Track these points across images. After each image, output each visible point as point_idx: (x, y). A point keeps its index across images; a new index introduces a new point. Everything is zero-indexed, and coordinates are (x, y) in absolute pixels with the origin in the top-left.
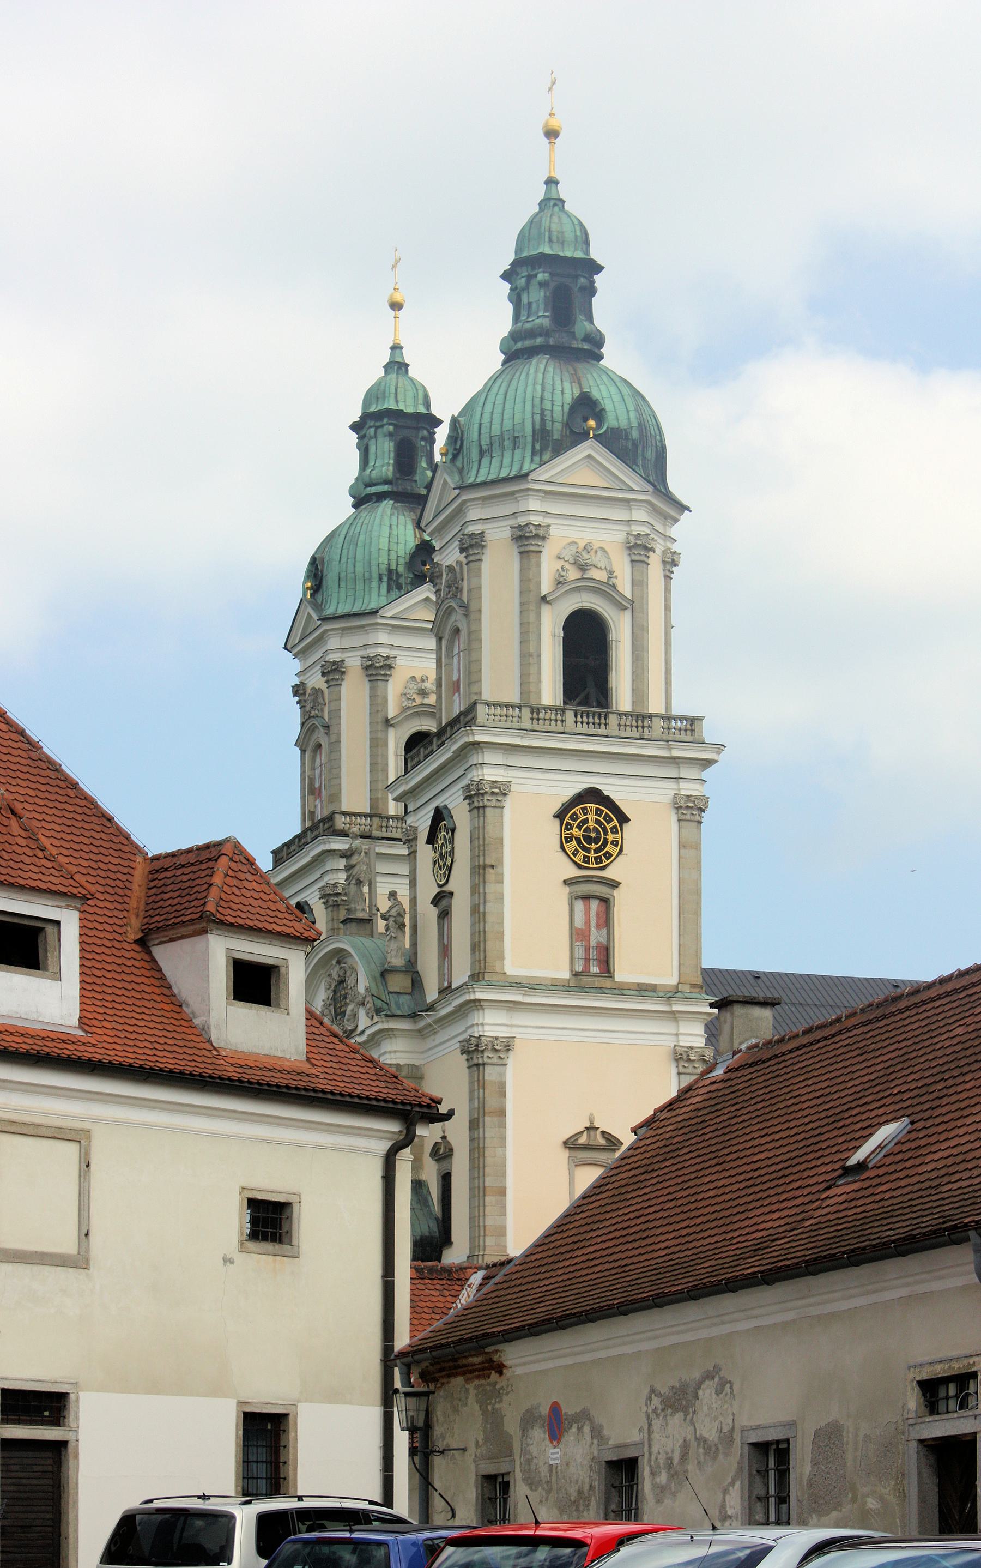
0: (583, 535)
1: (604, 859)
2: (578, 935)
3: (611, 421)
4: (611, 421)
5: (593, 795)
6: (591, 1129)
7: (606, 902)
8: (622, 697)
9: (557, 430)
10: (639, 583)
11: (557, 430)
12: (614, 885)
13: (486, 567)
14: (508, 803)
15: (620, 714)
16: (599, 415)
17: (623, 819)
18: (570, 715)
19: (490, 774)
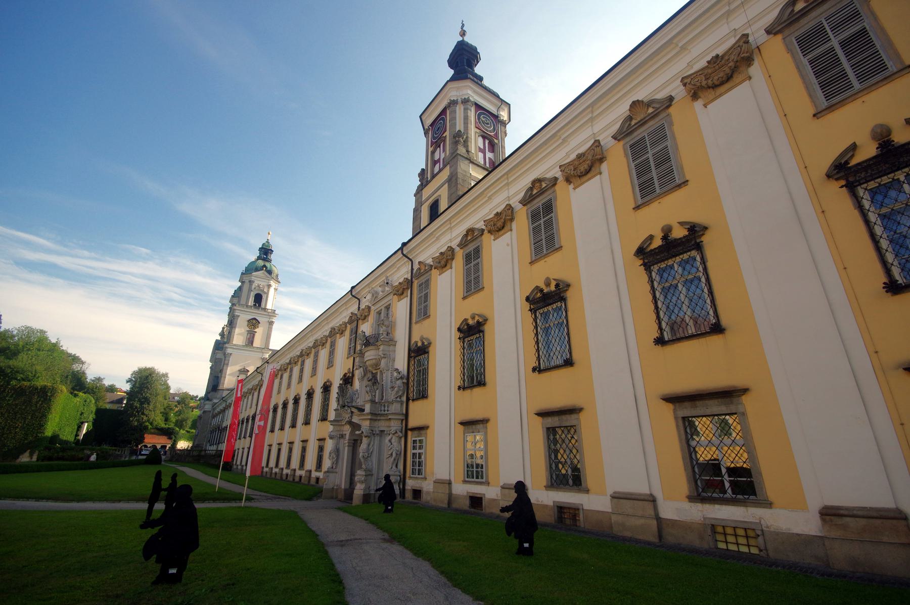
0: (260, 283)
1: (255, 328)
2: (249, 339)
3: (268, 269)
4: (268, 269)
5: (255, 319)
6: (244, 368)
7: (254, 335)
8: (263, 305)
9: (259, 269)
10: (268, 291)
11: (259, 269)
12: (256, 332)
13: (245, 285)
14: (239, 318)
15: (262, 308)
16: (266, 268)
18: (253, 308)
19: (236, 314)
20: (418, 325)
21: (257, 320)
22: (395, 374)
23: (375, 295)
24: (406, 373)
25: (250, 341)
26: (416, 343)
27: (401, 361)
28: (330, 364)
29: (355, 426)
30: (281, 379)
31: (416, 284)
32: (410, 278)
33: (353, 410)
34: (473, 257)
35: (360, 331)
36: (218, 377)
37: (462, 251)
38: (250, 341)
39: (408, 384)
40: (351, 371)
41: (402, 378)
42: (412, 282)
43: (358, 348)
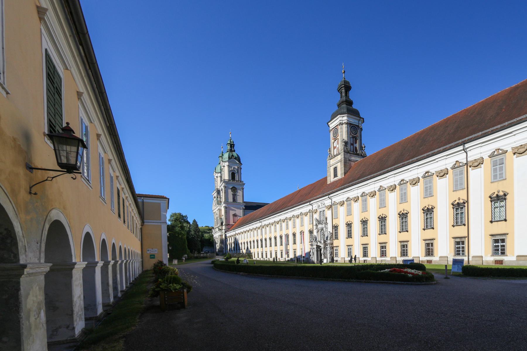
2: (233, 198)
17: (237, 189)
20: (335, 219)
21: (235, 187)
22: (329, 232)
23: (319, 206)
24: (332, 232)
25: (234, 200)
26: (334, 225)
27: (330, 229)
28: (302, 225)
29: (318, 247)
30: (275, 226)
31: (333, 206)
32: (331, 205)
33: (318, 242)
34: (349, 205)
35: (314, 217)
36: (222, 218)
37: (346, 202)
38: (234, 200)
39: (333, 235)
40: (312, 229)
41: (331, 234)
42: (332, 206)
43: (314, 223)
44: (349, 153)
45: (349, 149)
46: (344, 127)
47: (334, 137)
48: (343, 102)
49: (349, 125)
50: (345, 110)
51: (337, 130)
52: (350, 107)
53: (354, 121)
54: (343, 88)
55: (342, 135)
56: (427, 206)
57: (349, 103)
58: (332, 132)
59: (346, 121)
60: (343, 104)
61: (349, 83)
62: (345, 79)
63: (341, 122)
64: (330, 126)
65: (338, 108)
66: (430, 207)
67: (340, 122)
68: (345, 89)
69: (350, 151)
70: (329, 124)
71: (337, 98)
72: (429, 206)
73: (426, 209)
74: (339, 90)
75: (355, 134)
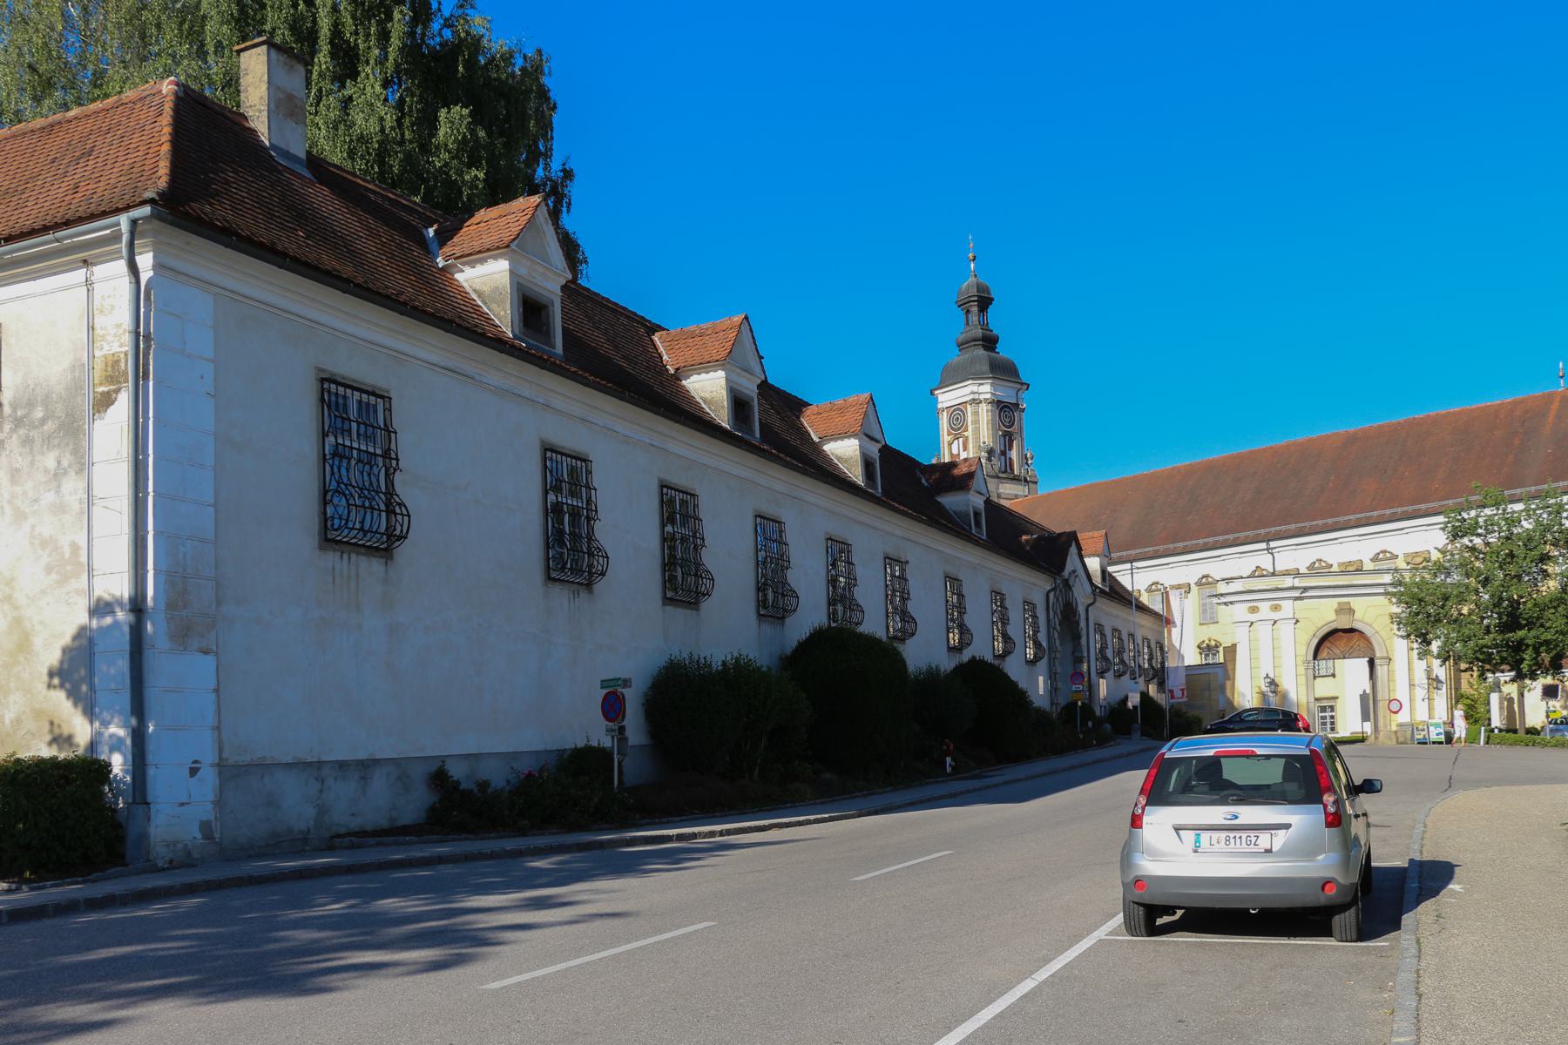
44: (998, 477)
45: (996, 468)
46: (983, 410)
47: (952, 428)
48: (975, 341)
49: (995, 405)
50: (986, 367)
51: (964, 414)
52: (994, 354)
53: (1007, 395)
54: (972, 303)
55: (977, 431)
56: (1207, 642)
57: (990, 342)
58: (945, 413)
59: (988, 396)
60: (974, 345)
61: (987, 290)
62: (975, 276)
63: (976, 396)
64: (941, 398)
65: (960, 350)
66: (1213, 643)
67: (972, 397)
68: (978, 306)
69: (1000, 471)
70: (936, 392)
71: (957, 325)
72: (1210, 641)
73: (1204, 645)
74: (963, 304)
75: (1009, 427)
